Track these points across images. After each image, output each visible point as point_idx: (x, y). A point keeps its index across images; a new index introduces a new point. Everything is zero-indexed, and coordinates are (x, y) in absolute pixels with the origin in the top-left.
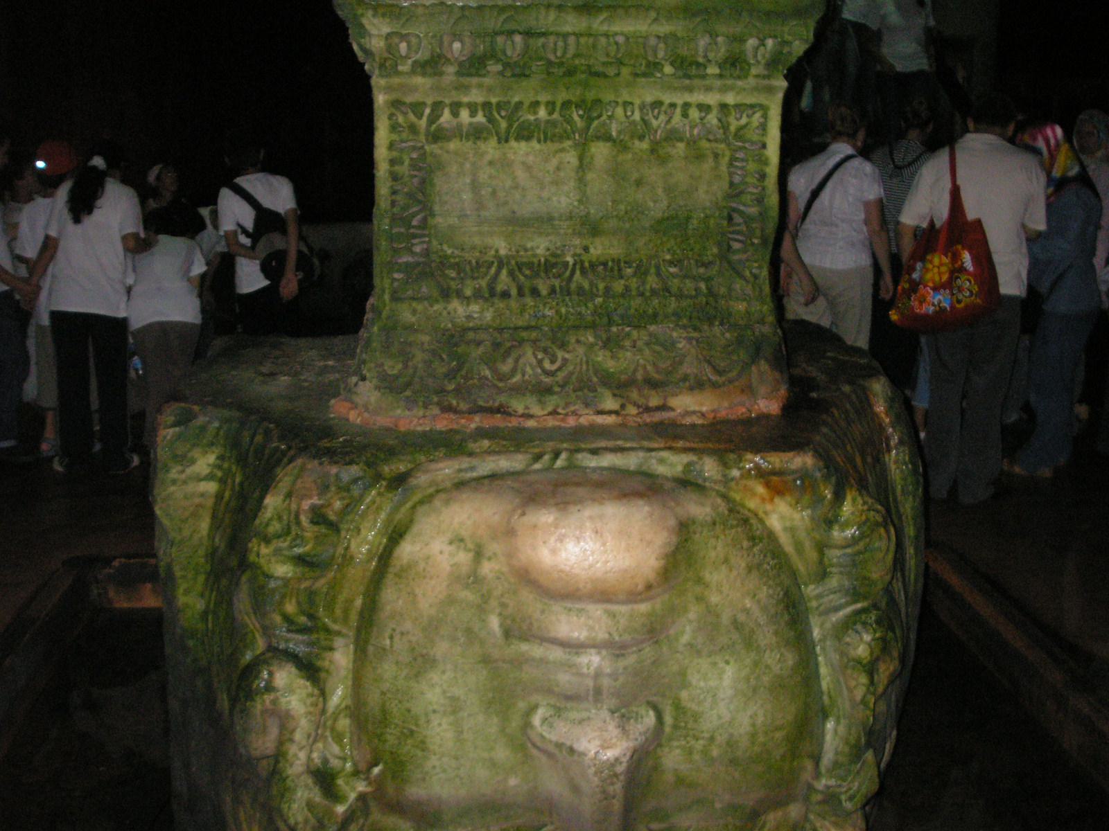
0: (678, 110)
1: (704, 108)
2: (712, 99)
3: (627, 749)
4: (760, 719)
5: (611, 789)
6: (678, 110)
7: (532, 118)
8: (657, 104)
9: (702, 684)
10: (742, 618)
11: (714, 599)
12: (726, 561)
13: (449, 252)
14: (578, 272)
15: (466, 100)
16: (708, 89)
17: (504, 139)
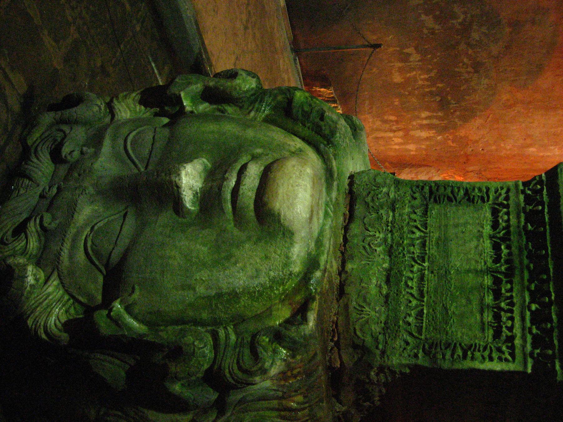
0: (509, 315)
1: (511, 329)
2: (517, 331)
3: (182, 183)
4: (170, 261)
5: (163, 174)
6: (509, 315)
7: (503, 247)
8: (512, 304)
9: (201, 235)
10: (233, 260)
11: (247, 246)
12: (267, 257)
13: (433, 212)
14: (420, 267)
15: (511, 217)
16: (523, 329)
17: (491, 237)
